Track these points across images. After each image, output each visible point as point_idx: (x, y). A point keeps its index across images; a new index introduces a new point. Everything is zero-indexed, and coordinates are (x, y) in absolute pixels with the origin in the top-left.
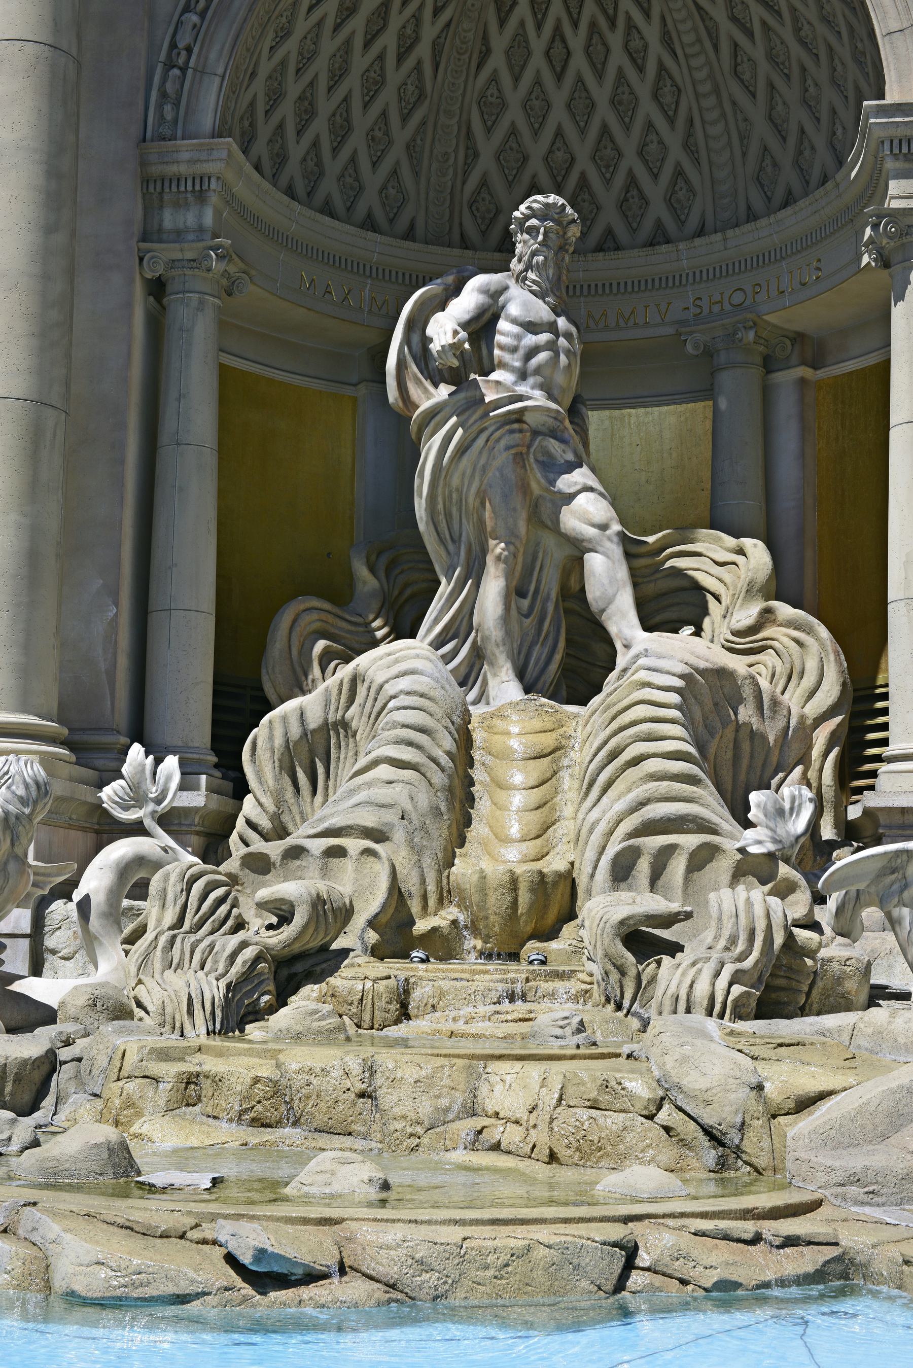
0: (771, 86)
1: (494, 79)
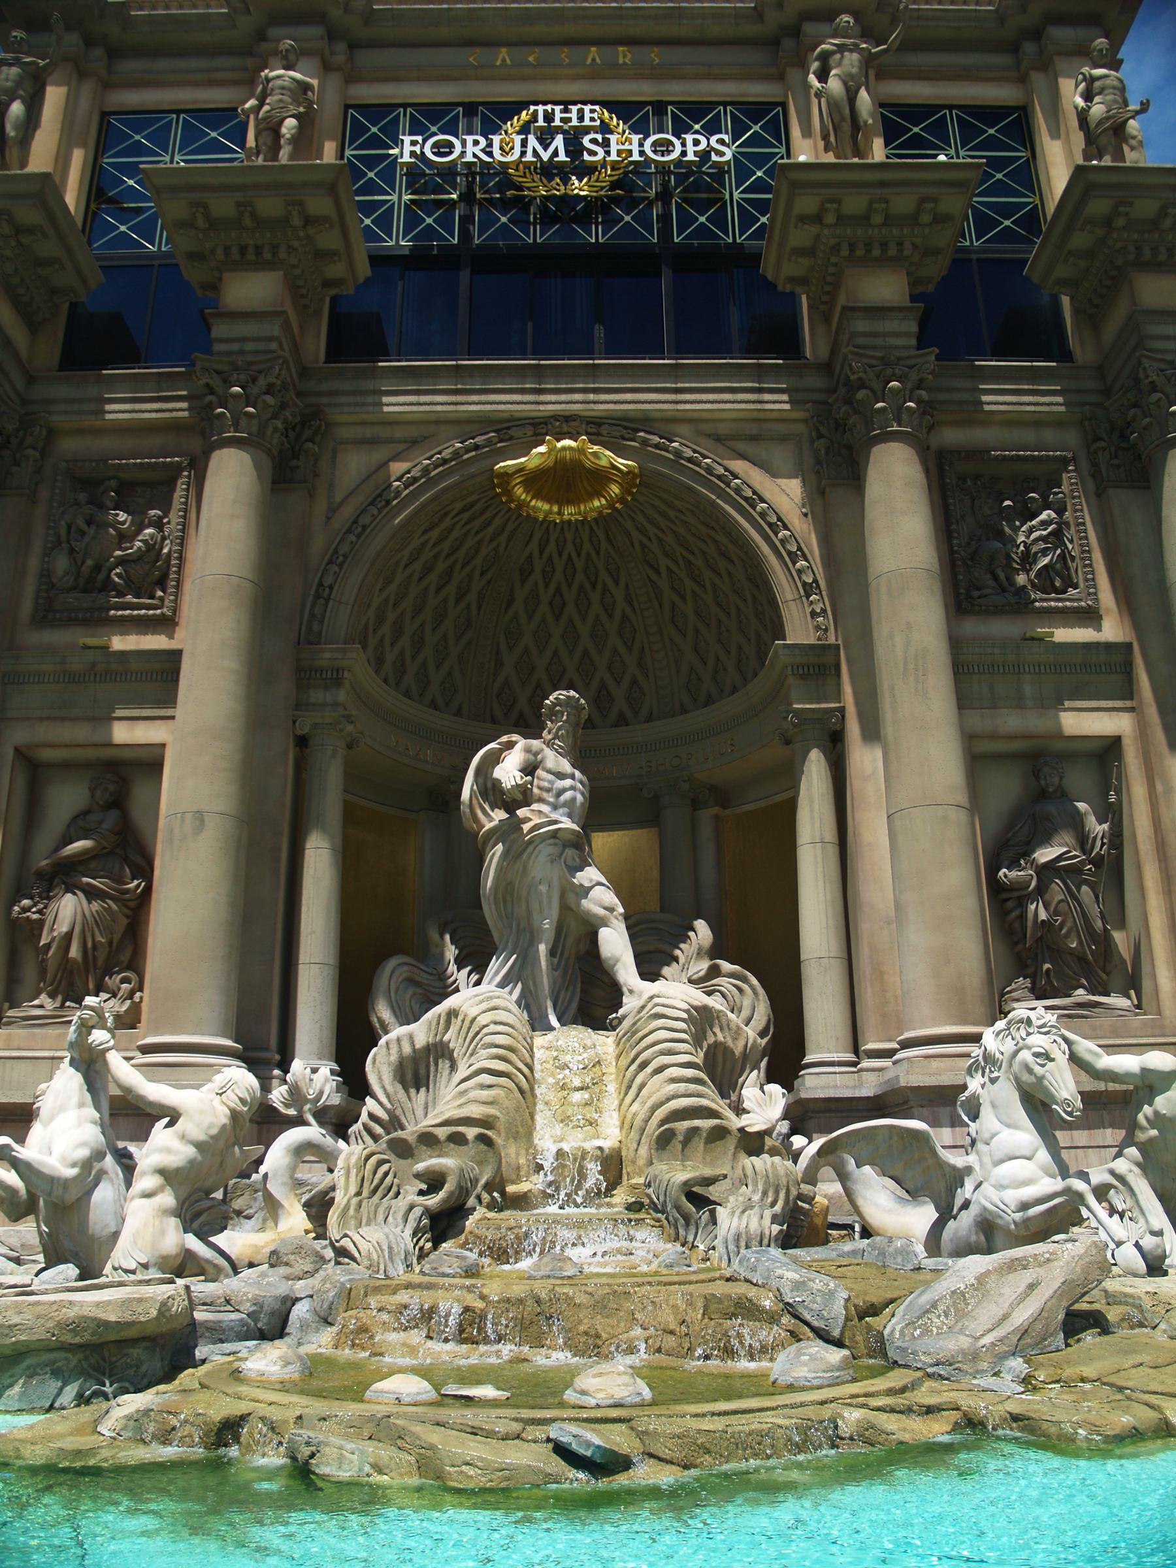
0: (697, 631)
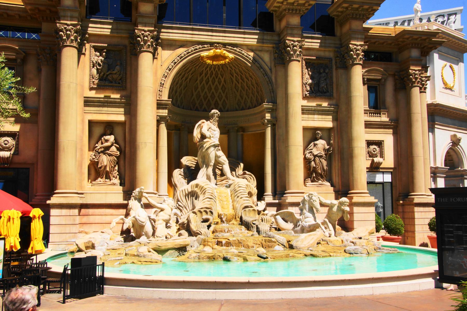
0: (241, 91)
1: (197, 84)
